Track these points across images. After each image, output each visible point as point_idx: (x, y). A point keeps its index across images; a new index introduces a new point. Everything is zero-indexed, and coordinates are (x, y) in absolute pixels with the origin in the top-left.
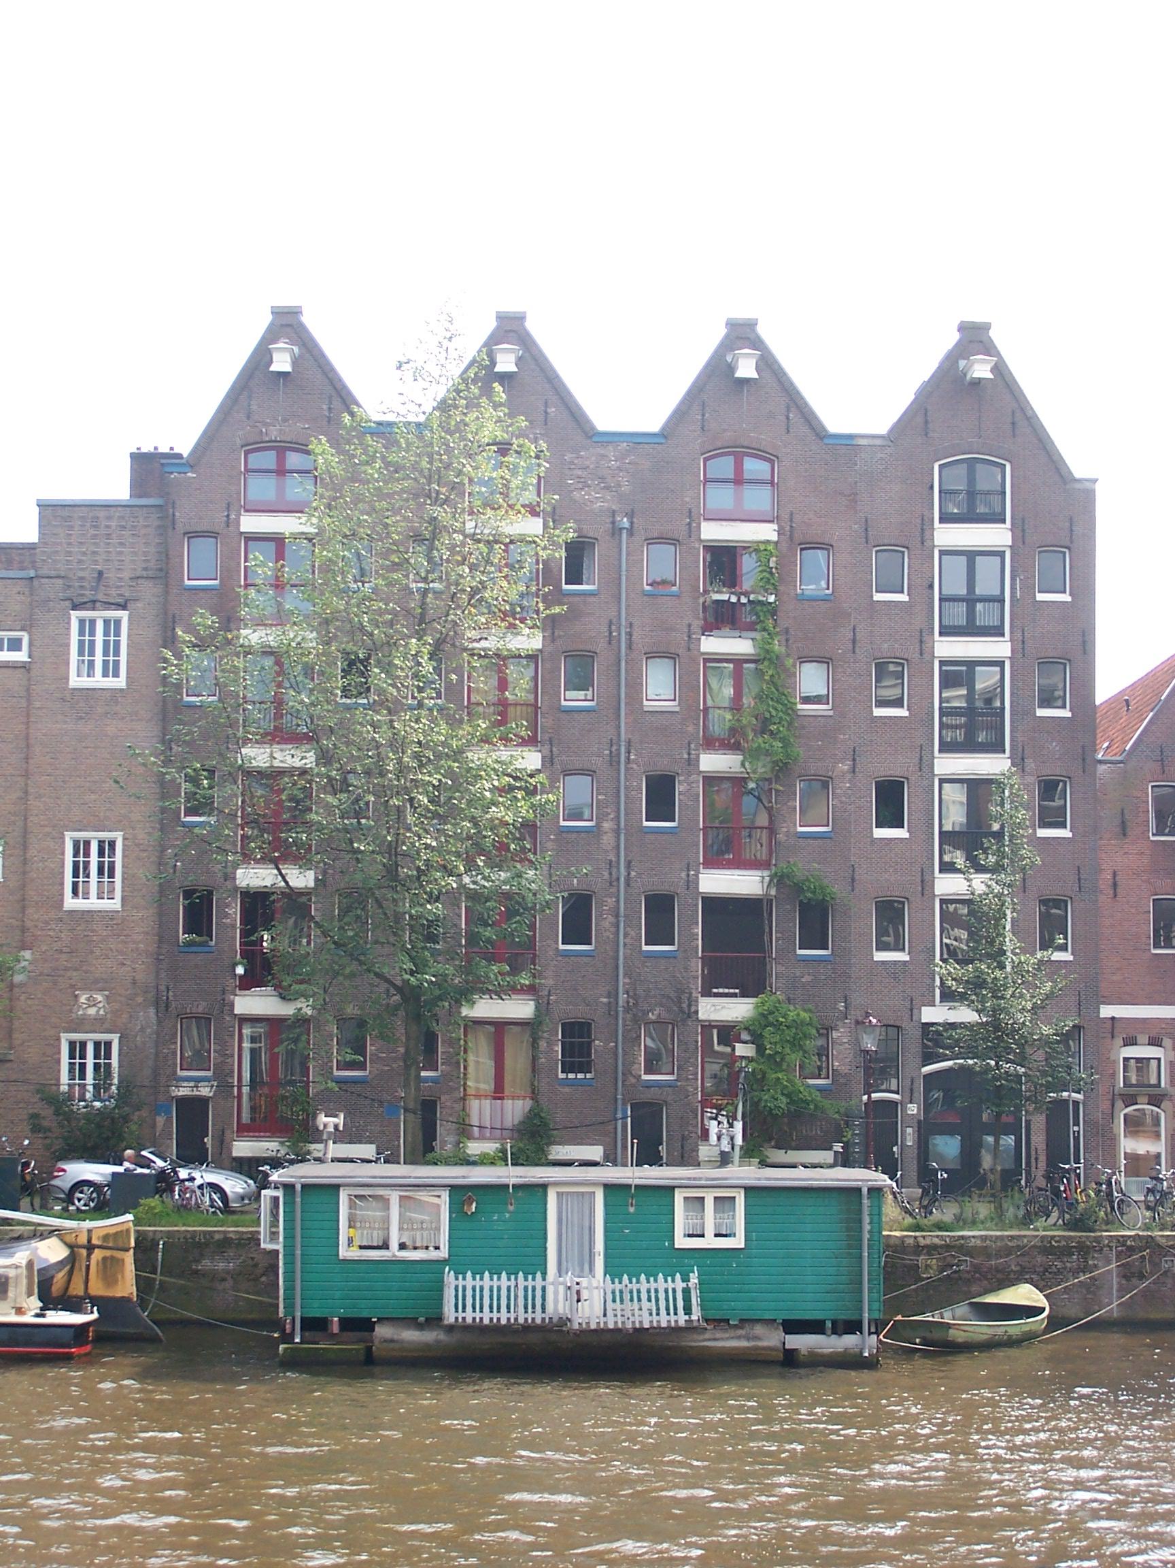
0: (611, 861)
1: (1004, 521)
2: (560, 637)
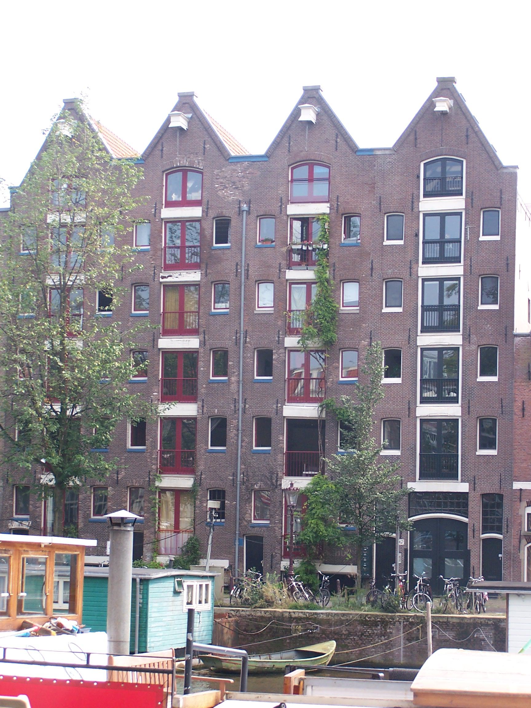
0: (235, 399)
1: (461, 194)
2: (210, 273)
